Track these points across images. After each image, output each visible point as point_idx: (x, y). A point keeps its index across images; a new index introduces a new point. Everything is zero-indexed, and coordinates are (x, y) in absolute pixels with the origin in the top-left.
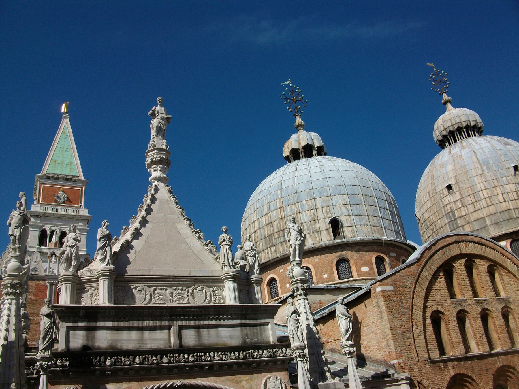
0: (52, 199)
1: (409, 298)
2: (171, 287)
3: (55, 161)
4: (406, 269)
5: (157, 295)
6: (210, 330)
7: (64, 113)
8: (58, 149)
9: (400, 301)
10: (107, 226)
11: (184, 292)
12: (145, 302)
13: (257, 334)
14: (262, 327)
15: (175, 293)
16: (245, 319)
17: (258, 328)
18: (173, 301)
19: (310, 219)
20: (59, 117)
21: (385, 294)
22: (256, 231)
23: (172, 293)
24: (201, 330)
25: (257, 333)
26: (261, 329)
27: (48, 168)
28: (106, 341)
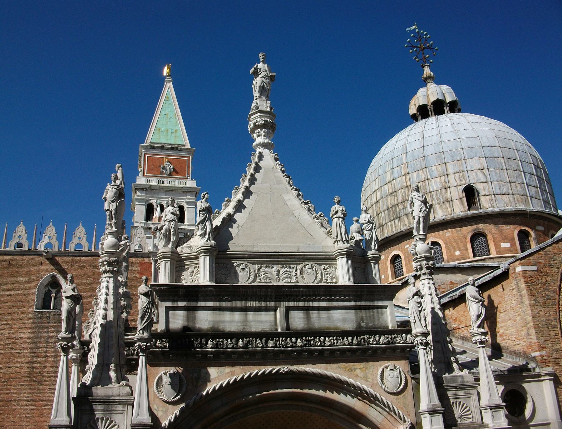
0: (158, 171)
1: (556, 280)
2: (277, 264)
3: (159, 129)
4: (554, 245)
5: (263, 273)
6: (321, 312)
7: (167, 76)
8: (162, 116)
9: (545, 283)
10: (207, 198)
11: (291, 270)
12: (249, 281)
13: (374, 318)
14: (380, 310)
15: (282, 271)
16: (360, 300)
17: (375, 310)
18: (279, 280)
19: (440, 187)
20: (161, 82)
21: (527, 275)
22: (377, 202)
23: (279, 271)
24: (311, 312)
25: (374, 316)
26: (378, 312)
27: (152, 137)
28: (207, 322)
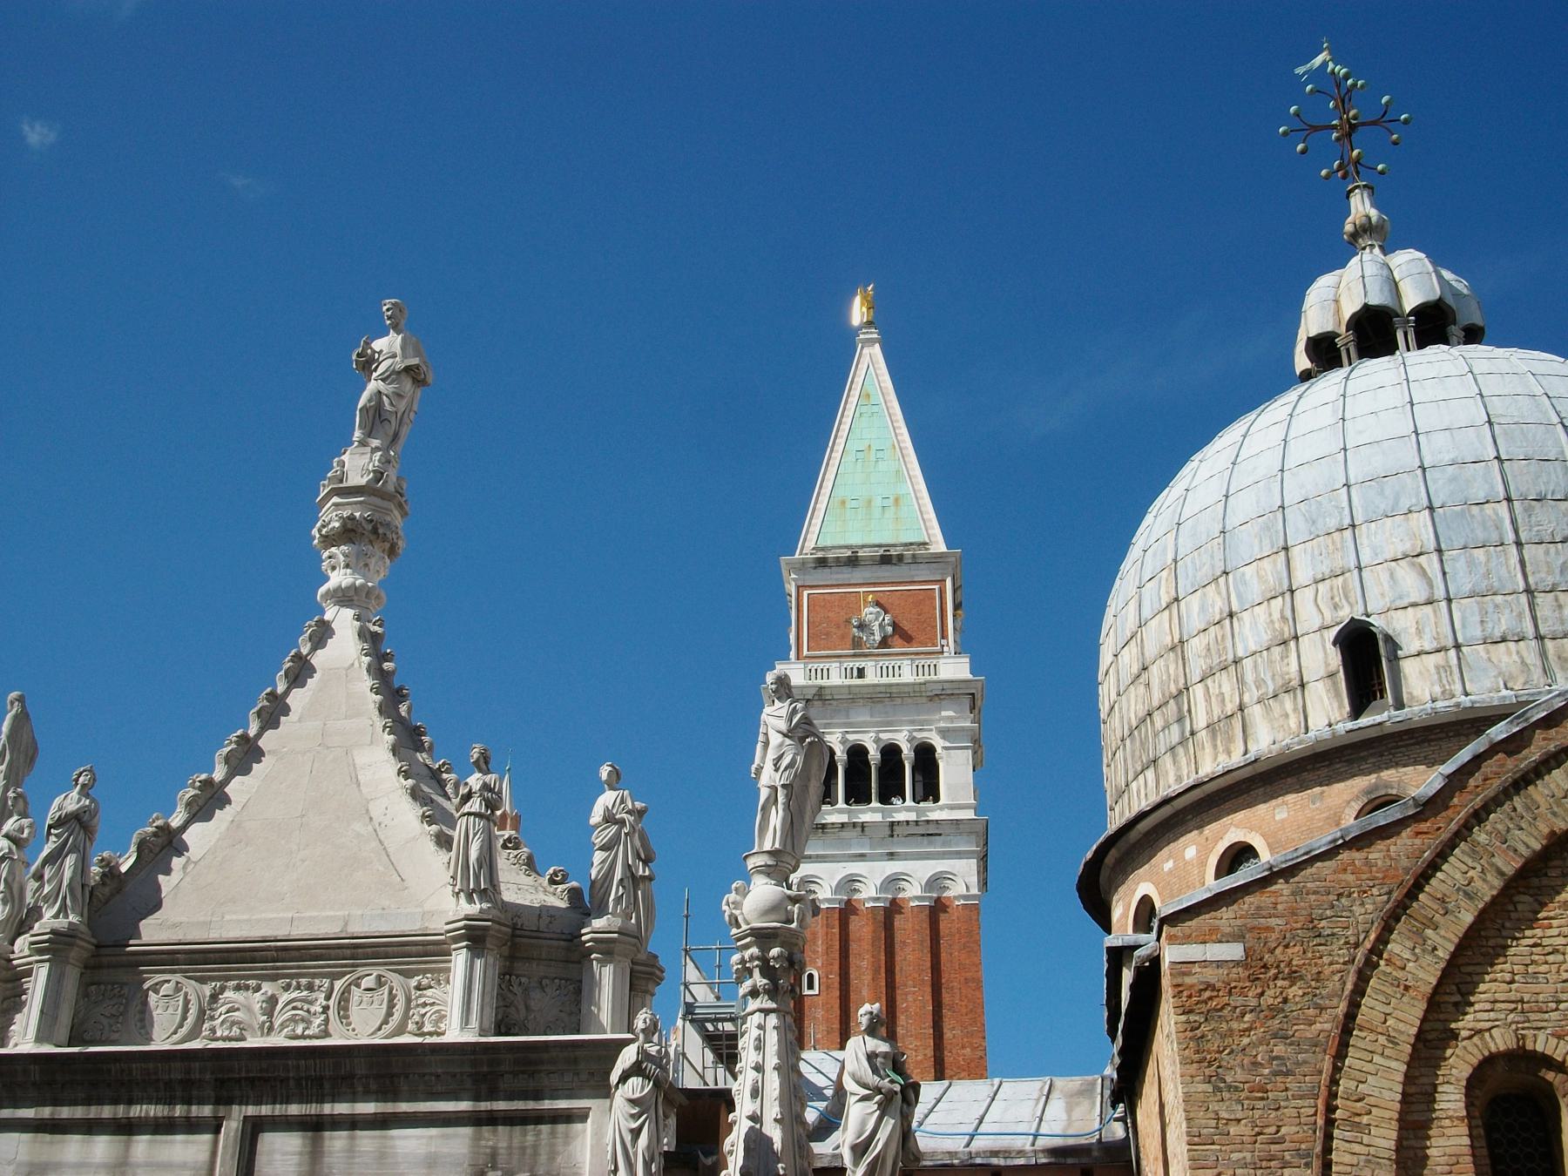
0: (843, 637)
1: (1330, 997)
2: (274, 978)
3: (843, 502)
4: (1345, 856)
5: (223, 1009)
6: (359, 1133)
7: (860, 328)
9: (1274, 1011)
10: (84, 786)
11: (314, 995)
12: (387, 1029)
13: (536, 1154)
14: (561, 1128)
15: (284, 997)
16: (492, 1096)
17: (545, 1128)
18: (271, 1029)
19: (1266, 638)
21: (1188, 980)
23: (272, 1001)
24: (327, 1134)
25: (535, 1147)
26: (553, 1134)
27: (826, 528)
28: (12, 1168)
